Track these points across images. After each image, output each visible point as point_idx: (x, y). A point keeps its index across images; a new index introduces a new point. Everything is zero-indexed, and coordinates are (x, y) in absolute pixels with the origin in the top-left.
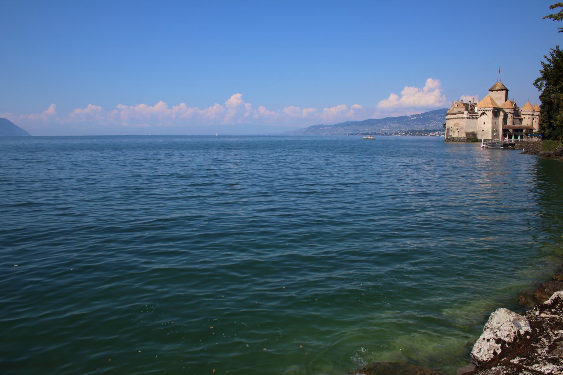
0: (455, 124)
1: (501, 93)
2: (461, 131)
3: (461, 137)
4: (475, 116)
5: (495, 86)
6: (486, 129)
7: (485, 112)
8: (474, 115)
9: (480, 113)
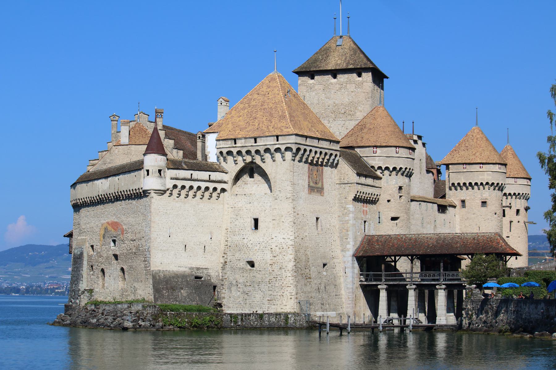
0: (106, 229)
1: (351, 87)
2: (131, 267)
3: (131, 303)
4: (203, 185)
5: (325, 52)
6: (268, 257)
7: (258, 160)
8: (197, 174)
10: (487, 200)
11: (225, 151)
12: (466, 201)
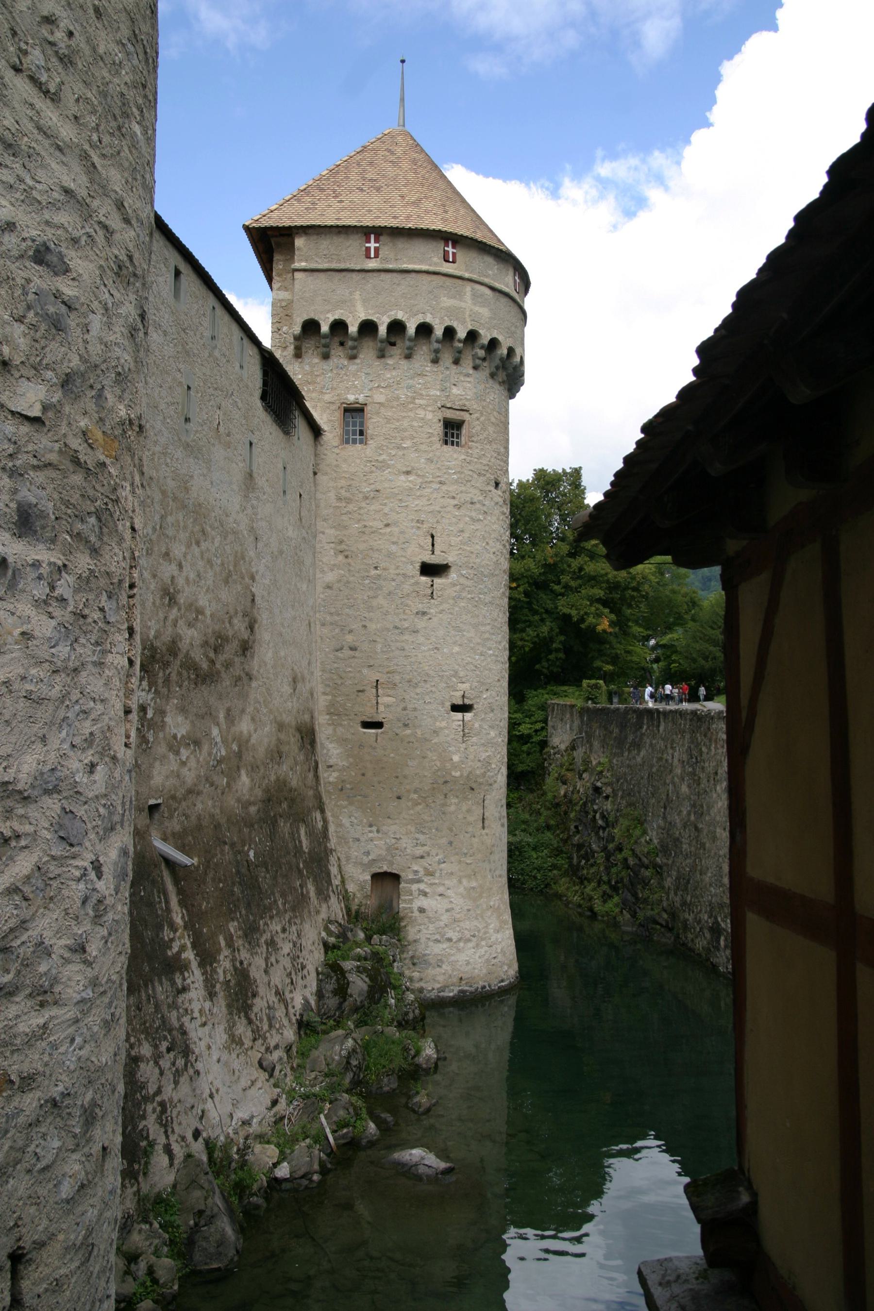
10: (465, 416)
12: (368, 409)
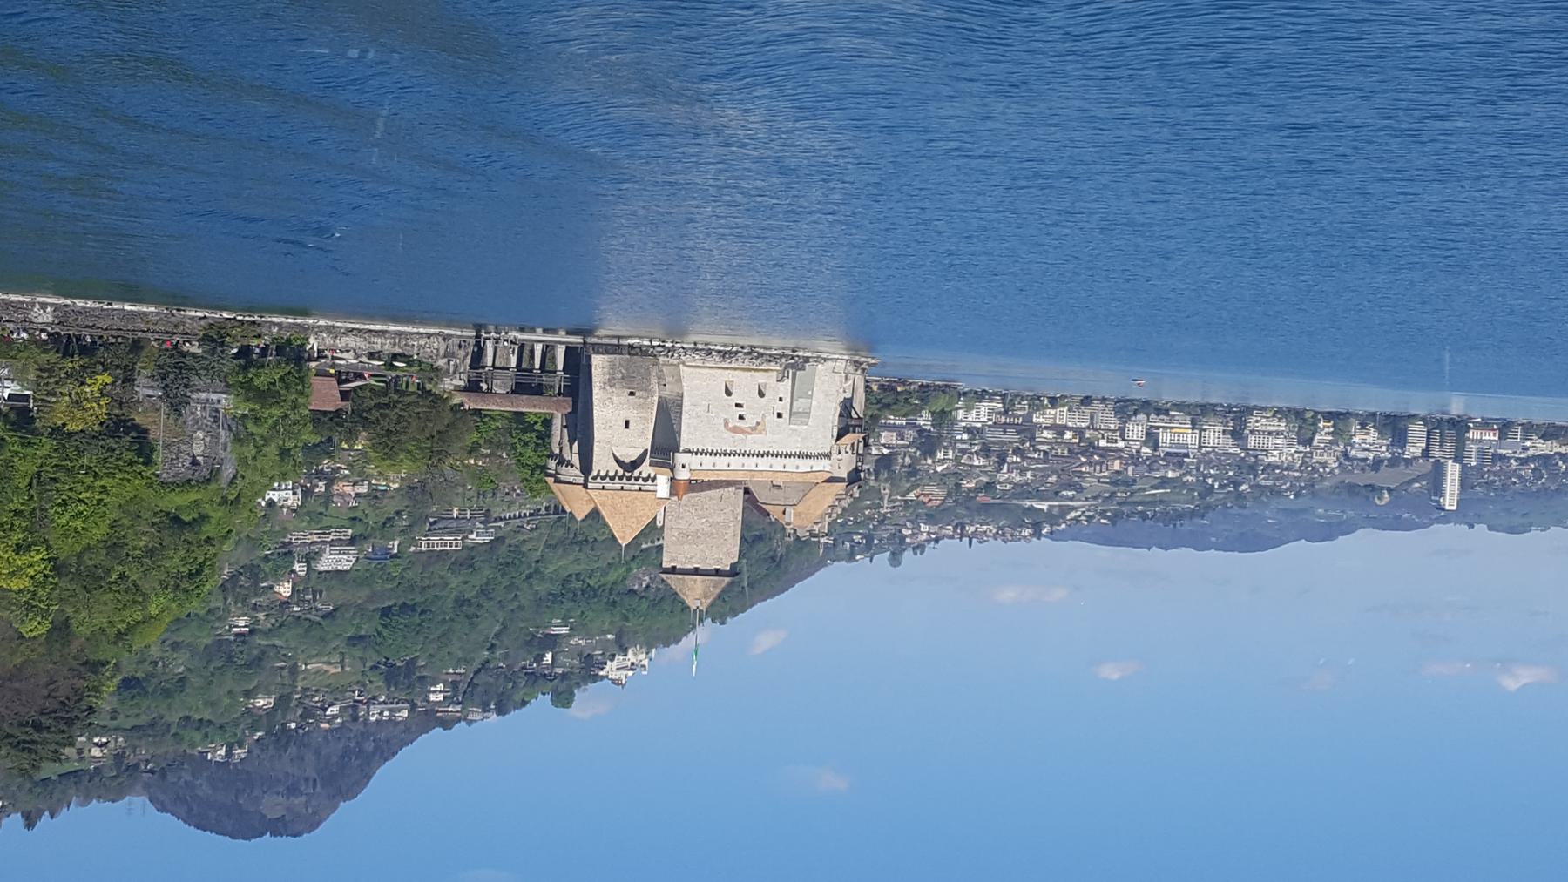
7: (621, 472)
9: (646, 469)
11: (650, 482)
